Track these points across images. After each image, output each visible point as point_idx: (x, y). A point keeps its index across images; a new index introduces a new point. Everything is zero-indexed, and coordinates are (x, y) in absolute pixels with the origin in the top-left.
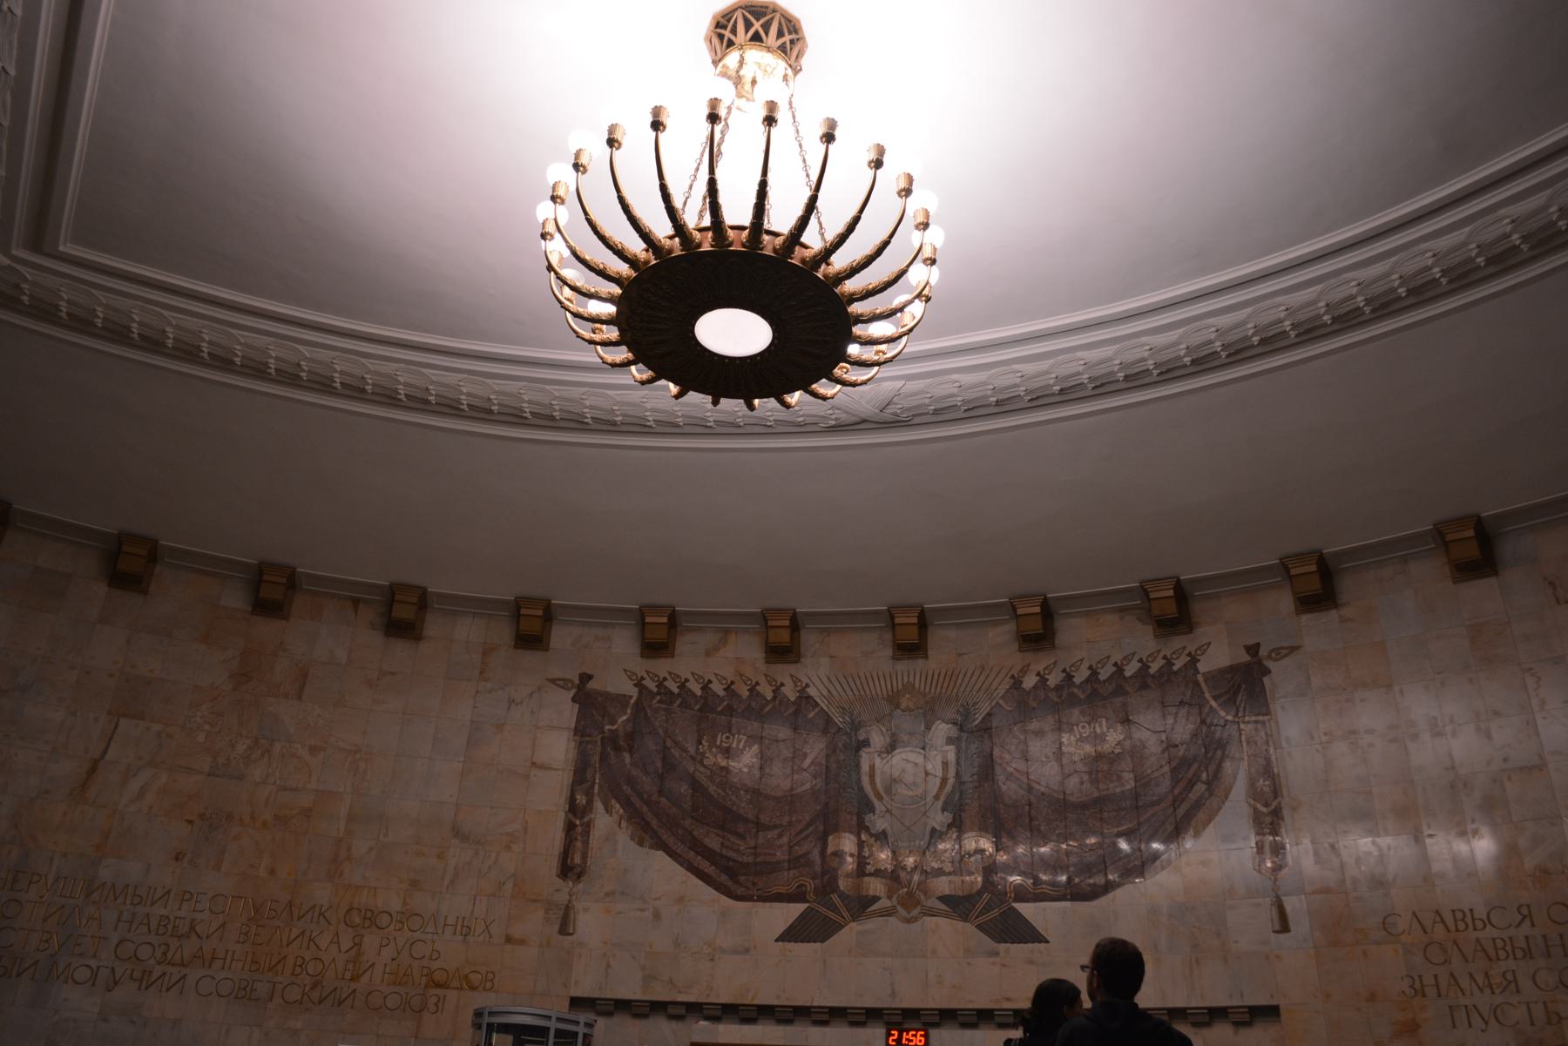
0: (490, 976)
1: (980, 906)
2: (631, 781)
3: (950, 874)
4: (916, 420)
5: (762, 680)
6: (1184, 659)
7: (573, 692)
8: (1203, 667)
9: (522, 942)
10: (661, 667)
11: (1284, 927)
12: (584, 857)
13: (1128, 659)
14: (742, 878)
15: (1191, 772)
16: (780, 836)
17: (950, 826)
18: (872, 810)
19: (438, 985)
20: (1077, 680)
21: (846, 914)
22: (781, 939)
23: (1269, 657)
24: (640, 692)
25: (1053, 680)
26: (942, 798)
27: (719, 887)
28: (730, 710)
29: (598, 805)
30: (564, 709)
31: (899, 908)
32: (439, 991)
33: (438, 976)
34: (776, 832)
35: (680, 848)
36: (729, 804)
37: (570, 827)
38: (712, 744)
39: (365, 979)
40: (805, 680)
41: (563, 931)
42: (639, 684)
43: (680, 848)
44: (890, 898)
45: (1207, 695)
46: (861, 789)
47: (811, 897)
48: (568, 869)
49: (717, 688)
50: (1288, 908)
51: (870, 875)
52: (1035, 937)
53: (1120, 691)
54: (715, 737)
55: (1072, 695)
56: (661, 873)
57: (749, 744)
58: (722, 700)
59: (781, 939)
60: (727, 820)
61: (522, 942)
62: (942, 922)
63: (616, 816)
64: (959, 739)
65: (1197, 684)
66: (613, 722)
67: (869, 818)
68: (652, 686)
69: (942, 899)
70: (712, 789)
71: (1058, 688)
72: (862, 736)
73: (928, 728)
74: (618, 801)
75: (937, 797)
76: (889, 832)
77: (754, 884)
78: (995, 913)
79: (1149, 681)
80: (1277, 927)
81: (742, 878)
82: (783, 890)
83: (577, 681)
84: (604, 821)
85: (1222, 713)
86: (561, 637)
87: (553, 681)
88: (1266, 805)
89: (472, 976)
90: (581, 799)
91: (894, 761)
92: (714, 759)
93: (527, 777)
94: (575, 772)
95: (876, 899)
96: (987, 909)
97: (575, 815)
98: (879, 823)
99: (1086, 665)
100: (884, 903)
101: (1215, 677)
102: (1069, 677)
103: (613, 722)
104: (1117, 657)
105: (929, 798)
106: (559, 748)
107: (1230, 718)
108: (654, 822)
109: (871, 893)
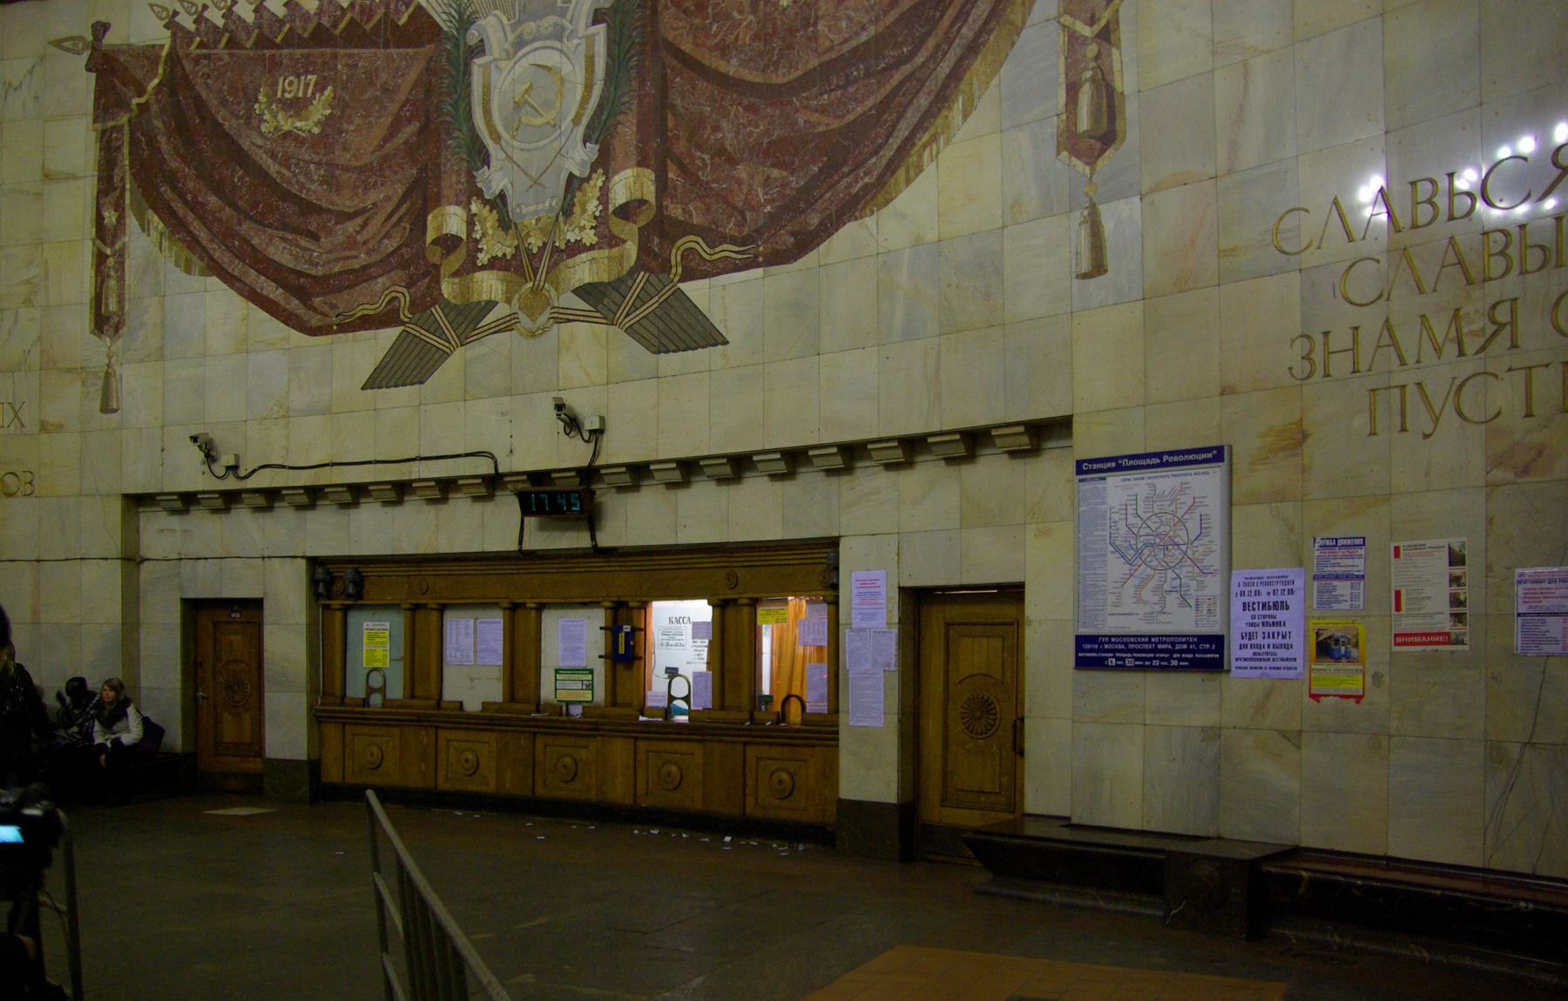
0: (29, 477)
1: (631, 297)
2: (173, 180)
3: (592, 247)
7: (87, 54)
12: (121, 301)
14: (317, 301)
16: (364, 225)
17: (593, 169)
18: (486, 162)
21: (451, 335)
22: (372, 383)
24: (174, 35)
26: (585, 121)
27: (288, 319)
28: (289, 42)
29: (132, 222)
30: (78, 84)
31: (524, 319)
34: (359, 220)
35: (237, 268)
36: (295, 190)
37: (100, 259)
42: (172, 25)
43: (237, 268)
44: (509, 301)
46: (472, 128)
47: (405, 315)
51: (483, 268)
52: (713, 338)
54: (274, 84)
56: (211, 310)
57: (319, 87)
58: (282, 22)
59: (372, 383)
62: (581, 328)
63: (155, 235)
66: (141, 92)
67: (482, 175)
68: (187, 21)
69: (583, 291)
70: (273, 168)
72: (473, 36)
74: (156, 211)
75: (576, 121)
76: (509, 194)
77: (333, 307)
78: (653, 304)
81: (317, 301)
82: (369, 310)
83: (90, 38)
84: (143, 241)
87: (58, 44)
90: (110, 217)
91: (518, 70)
92: (274, 121)
93: (39, 196)
94: (100, 179)
95: (491, 305)
96: (641, 300)
97: (104, 241)
98: (494, 179)
103: (141, 92)
105: (567, 123)
106: (77, 145)
108: (203, 235)
109: (485, 297)
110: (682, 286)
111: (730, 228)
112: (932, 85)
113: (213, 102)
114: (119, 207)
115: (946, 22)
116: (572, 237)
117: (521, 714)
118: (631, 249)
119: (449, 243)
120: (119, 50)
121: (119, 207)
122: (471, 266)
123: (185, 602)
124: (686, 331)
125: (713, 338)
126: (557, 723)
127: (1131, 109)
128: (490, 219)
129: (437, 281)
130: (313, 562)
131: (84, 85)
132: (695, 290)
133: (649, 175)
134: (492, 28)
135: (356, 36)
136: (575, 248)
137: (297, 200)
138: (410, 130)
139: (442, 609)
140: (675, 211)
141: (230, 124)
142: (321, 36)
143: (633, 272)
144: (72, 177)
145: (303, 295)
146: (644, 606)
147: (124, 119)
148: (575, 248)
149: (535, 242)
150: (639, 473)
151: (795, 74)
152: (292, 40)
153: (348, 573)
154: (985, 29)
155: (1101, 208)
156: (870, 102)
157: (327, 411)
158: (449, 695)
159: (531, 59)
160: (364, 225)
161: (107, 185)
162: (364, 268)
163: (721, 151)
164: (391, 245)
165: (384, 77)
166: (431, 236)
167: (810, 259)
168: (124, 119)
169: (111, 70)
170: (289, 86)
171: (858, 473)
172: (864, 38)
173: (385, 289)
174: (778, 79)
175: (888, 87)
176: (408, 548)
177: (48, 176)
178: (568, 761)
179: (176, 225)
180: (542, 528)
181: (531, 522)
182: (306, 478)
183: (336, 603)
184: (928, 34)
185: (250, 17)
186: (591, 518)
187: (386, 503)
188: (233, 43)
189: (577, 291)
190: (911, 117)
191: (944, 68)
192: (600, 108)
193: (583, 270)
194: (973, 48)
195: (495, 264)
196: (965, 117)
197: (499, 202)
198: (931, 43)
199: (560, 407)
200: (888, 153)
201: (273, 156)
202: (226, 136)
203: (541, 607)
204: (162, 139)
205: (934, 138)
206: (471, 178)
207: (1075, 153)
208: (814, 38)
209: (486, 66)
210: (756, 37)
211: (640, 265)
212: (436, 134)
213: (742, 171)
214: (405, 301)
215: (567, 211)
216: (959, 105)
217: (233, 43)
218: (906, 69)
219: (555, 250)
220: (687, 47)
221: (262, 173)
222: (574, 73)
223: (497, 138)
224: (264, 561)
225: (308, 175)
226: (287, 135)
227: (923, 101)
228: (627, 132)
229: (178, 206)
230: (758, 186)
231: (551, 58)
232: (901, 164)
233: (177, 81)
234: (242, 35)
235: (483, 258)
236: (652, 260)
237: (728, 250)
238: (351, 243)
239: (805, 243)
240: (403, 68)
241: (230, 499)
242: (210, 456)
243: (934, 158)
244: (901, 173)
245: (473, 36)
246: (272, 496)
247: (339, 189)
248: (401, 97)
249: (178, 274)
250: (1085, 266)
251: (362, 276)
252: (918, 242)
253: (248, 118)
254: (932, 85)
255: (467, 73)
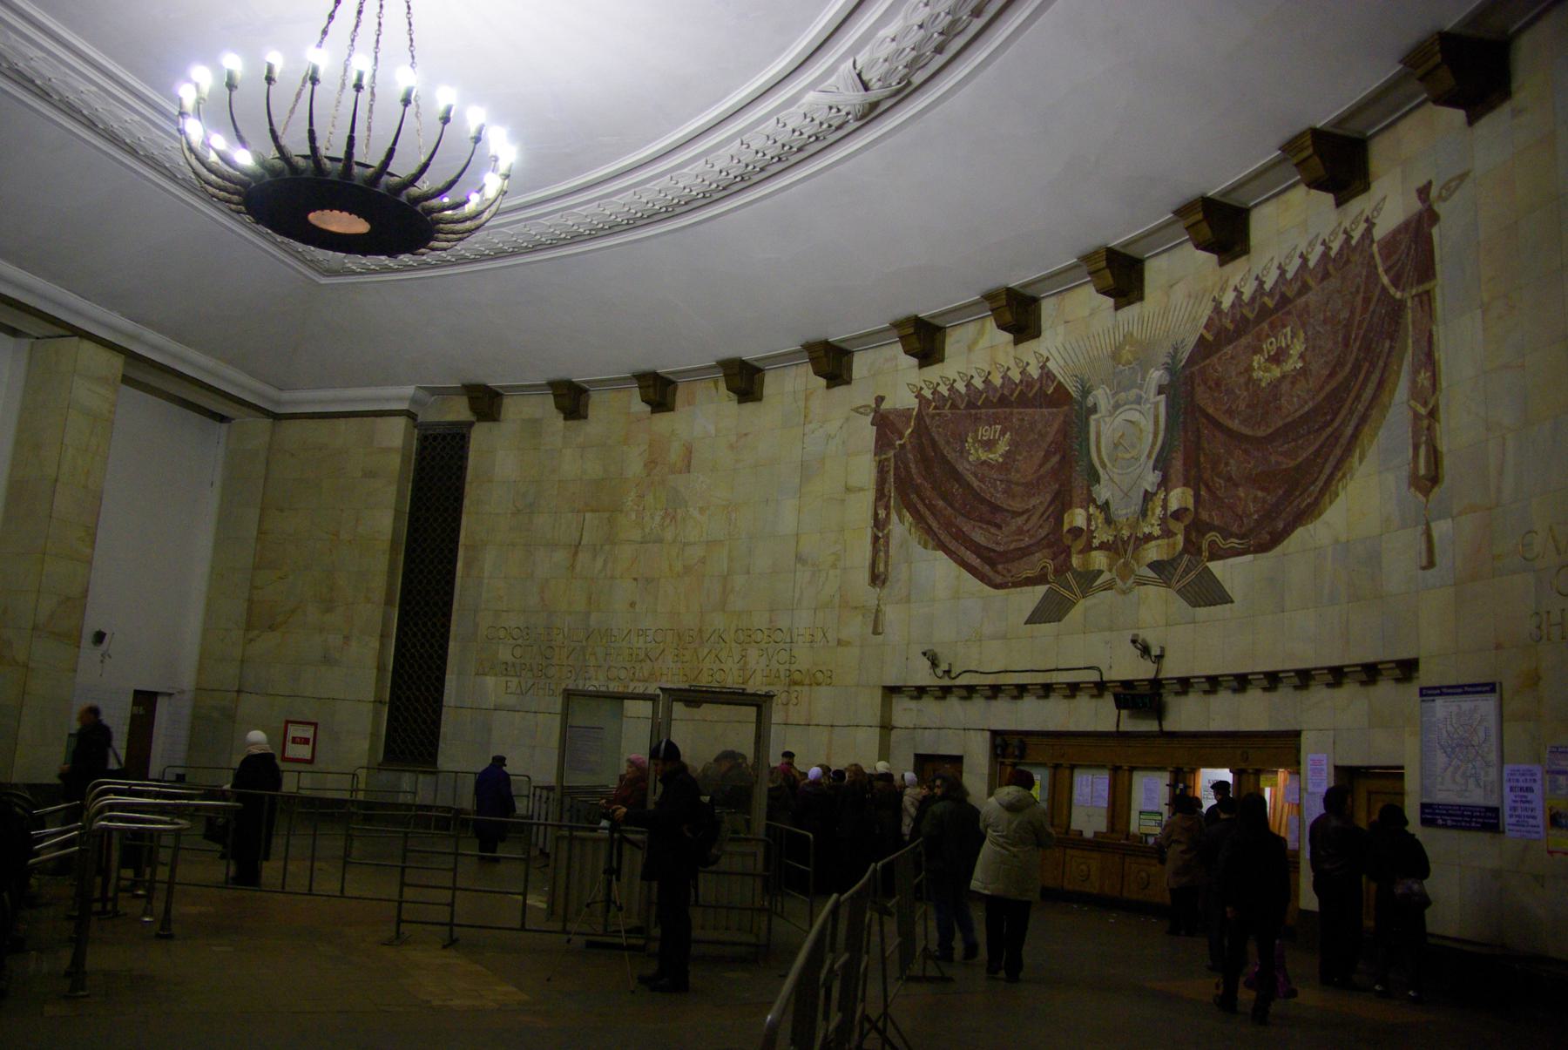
1: (1180, 570)
2: (918, 490)
3: (1157, 538)
4: (917, 79)
5: (1012, 363)
6: (1363, 226)
8: (1379, 233)
9: (848, 644)
10: (934, 373)
11: (1431, 564)
13: (1311, 244)
15: (1361, 377)
16: (1027, 520)
17: (1159, 486)
18: (1098, 481)
19: (796, 683)
20: (1267, 287)
22: (1029, 622)
23: (1441, 198)
25: (1247, 292)
28: (985, 405)
29: (894, 517)
31: (1118, 580)
32: (797, 688)
33: (797, 676)
35: (953, 545)
37: (876, 539)
38: (975, 440)
39: (751, 682)
40: (1046, 354)
41: (876, 632)
42: (919, 396)
43: (953, 545)
45: (1380, 270)
47: (1051, 577)
48: (877, 579)
49: (978, 383)
50: (1435, 535)
52: (1222, 598)
53: (1305, 288)
54: (976, 432)
55: (1264, 305)
57: (1003, 433)
58: (981, 393)
59: (1029, 622)
60: (992, 514)
61: (848, 644)
62: (1151, 589)
64: (1171, 384)
65: (1372, 256)
68: (927, 393)
69: (1152, 566)
70: (976, 484)
71: (1253, 299)
73: (1143, 379)
75: (1149, 457)
78: (1192, 575)
79: (1330, 268)
80: (1424, 562)
82: (1030, 573)
84: (900, 528)
85: (1392, 290)
86: (861, 364)
87: (856, 410)
88: (1425, 404)
89: (819, 675)
90: (882, 513)
92: (977, 454)
95: (1100, 572)
96: (1187, 572)
98: (1103, 492)
99: (1276, 263)
100: (1105, 577)
101: (1390, 244)
102: (1261, 283)
104: (1302, 247)
106: (864, 470)
107: (1398, 295)
108: (934, 525)
110: (1211, 565)
111: (1235, 529)
112: (1343, 441)
113: (941, 443)
114: (887, 508)
115: (1350, 400)
116: (1147, 530)
117: (1117, 842)
118: (1180, 538)
119: (1076, 532)
120: (889, 412)
121: (887, 508)
122: (1089, 548)
123: (917, 756)
124: (1209, 594)
125: (1227, 600)
126: (1135, 848)
127: (1446, 462)
128: (1100, 517)
129: (1069, 556)
130: (995, 734)
131: (870, 433)
132: (1216, 567)
133: (1190, 492)
134: (1101, 396)
135: (1023, 401)
136: (1149, 538)
137: (990, 503)
138: (1055, 459)
139: (1072, 768)
140: (1204, 516)
141: (951, 456)
142: (1003, 401)
143: (1181, 554)
144: (861, 489)
145: (992, 563)
146: (1194, 771)
147: (891, 454)
148: (1149, 538)
149: (1125, 533)
150: (1185, 684)
151: (1270, 431)
152: (988, 403)
153: (1015, 741)
154: (1369, 408)
155: (1433, 525)
156: (1311, 449)
157: (1004, 637)
158: (1076, 824)
159: (1123, 416)
160: (1027, 520)
161: (881, 494)
162: (1028, 547)
163: (1230, 479)
164: (1043, 532)
165: (1040, 426)
166: (1066, 527)
167: (1279, 549)
168: (891, 454)
169: (885, 423)
170: (985, 432)
171: (1312, 689)
172: (1306, 408)
173: (1041, 560)
174: (1260, 433)
175: (1317, 444)
176: (1051, 727)
177: (848, 489)
178: (1143, 874)
179: (919, 518)
180: (1131, 716)
181: (1124, 713)
182: (990, 680)
183: (1008, 761)
184: (1340, 409)
185: (963, 390)
186: (1159, 712)
187: (1039, 697)
188: (954, 406)
189: (1152, 566)
190: (1332, 460)
191: (1349, 431)
192: (1162, 449)
193: (1153, 552)
194: (1364, 419)
195: (1103, 546)
196: (1361, 460)
197: (1105, 507)
198: (1344, 412)
199: (1134, 642)
200: (1320, 483)
201: (976, 475)
202: (949, 462)
203: (1132, 769)
204: (912, 466)
205: (1344, 476)
206: (1090, 491)
207: (1418, 488)
208: (1279, 408)
209: (1097, 421)
210: (1248, 406)
211: (1185, 550)
212: (1068, 465)
213: (1241, 492)
214: (1051, 569)
215: (1144, 513)
216: (1357, 454)
217: (954, 406)
218: (1329, 430)
219: (1137, 538)
220: (1210, 411)
221: (969, 485)
222: (1148, 426)
223: (1104, 466)
224: (965, 732)
225: (995, 487)
226: (984, 463)
227: (1338, 451)
228: (1178, 464)
229: (920, 507)
230: (1250, 501)
231: (1135, 416)
232: (1327, 490)
233: (922, 430)
234: (959, 401)
235: (1096, 542)
236: (1191, 547)
237: (1234, 542)
238: (1020, 531)
239: (1276, 539)
240: (1048, 421)
241: (946, 691)
242: (934, 664)
243: (1344, 488)
244: (1327, 498)
245: (1090, 401)
246: (970, 691)
247: (1014, 497)
248: (1049, 439)
249: (919, 548)
250: (1424, 563)
251: (1025, 552)
252: (1337, 541)
253: (961, 452)
254: (1343, 441)
255: (1087, 424)
